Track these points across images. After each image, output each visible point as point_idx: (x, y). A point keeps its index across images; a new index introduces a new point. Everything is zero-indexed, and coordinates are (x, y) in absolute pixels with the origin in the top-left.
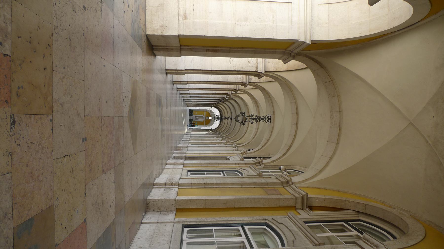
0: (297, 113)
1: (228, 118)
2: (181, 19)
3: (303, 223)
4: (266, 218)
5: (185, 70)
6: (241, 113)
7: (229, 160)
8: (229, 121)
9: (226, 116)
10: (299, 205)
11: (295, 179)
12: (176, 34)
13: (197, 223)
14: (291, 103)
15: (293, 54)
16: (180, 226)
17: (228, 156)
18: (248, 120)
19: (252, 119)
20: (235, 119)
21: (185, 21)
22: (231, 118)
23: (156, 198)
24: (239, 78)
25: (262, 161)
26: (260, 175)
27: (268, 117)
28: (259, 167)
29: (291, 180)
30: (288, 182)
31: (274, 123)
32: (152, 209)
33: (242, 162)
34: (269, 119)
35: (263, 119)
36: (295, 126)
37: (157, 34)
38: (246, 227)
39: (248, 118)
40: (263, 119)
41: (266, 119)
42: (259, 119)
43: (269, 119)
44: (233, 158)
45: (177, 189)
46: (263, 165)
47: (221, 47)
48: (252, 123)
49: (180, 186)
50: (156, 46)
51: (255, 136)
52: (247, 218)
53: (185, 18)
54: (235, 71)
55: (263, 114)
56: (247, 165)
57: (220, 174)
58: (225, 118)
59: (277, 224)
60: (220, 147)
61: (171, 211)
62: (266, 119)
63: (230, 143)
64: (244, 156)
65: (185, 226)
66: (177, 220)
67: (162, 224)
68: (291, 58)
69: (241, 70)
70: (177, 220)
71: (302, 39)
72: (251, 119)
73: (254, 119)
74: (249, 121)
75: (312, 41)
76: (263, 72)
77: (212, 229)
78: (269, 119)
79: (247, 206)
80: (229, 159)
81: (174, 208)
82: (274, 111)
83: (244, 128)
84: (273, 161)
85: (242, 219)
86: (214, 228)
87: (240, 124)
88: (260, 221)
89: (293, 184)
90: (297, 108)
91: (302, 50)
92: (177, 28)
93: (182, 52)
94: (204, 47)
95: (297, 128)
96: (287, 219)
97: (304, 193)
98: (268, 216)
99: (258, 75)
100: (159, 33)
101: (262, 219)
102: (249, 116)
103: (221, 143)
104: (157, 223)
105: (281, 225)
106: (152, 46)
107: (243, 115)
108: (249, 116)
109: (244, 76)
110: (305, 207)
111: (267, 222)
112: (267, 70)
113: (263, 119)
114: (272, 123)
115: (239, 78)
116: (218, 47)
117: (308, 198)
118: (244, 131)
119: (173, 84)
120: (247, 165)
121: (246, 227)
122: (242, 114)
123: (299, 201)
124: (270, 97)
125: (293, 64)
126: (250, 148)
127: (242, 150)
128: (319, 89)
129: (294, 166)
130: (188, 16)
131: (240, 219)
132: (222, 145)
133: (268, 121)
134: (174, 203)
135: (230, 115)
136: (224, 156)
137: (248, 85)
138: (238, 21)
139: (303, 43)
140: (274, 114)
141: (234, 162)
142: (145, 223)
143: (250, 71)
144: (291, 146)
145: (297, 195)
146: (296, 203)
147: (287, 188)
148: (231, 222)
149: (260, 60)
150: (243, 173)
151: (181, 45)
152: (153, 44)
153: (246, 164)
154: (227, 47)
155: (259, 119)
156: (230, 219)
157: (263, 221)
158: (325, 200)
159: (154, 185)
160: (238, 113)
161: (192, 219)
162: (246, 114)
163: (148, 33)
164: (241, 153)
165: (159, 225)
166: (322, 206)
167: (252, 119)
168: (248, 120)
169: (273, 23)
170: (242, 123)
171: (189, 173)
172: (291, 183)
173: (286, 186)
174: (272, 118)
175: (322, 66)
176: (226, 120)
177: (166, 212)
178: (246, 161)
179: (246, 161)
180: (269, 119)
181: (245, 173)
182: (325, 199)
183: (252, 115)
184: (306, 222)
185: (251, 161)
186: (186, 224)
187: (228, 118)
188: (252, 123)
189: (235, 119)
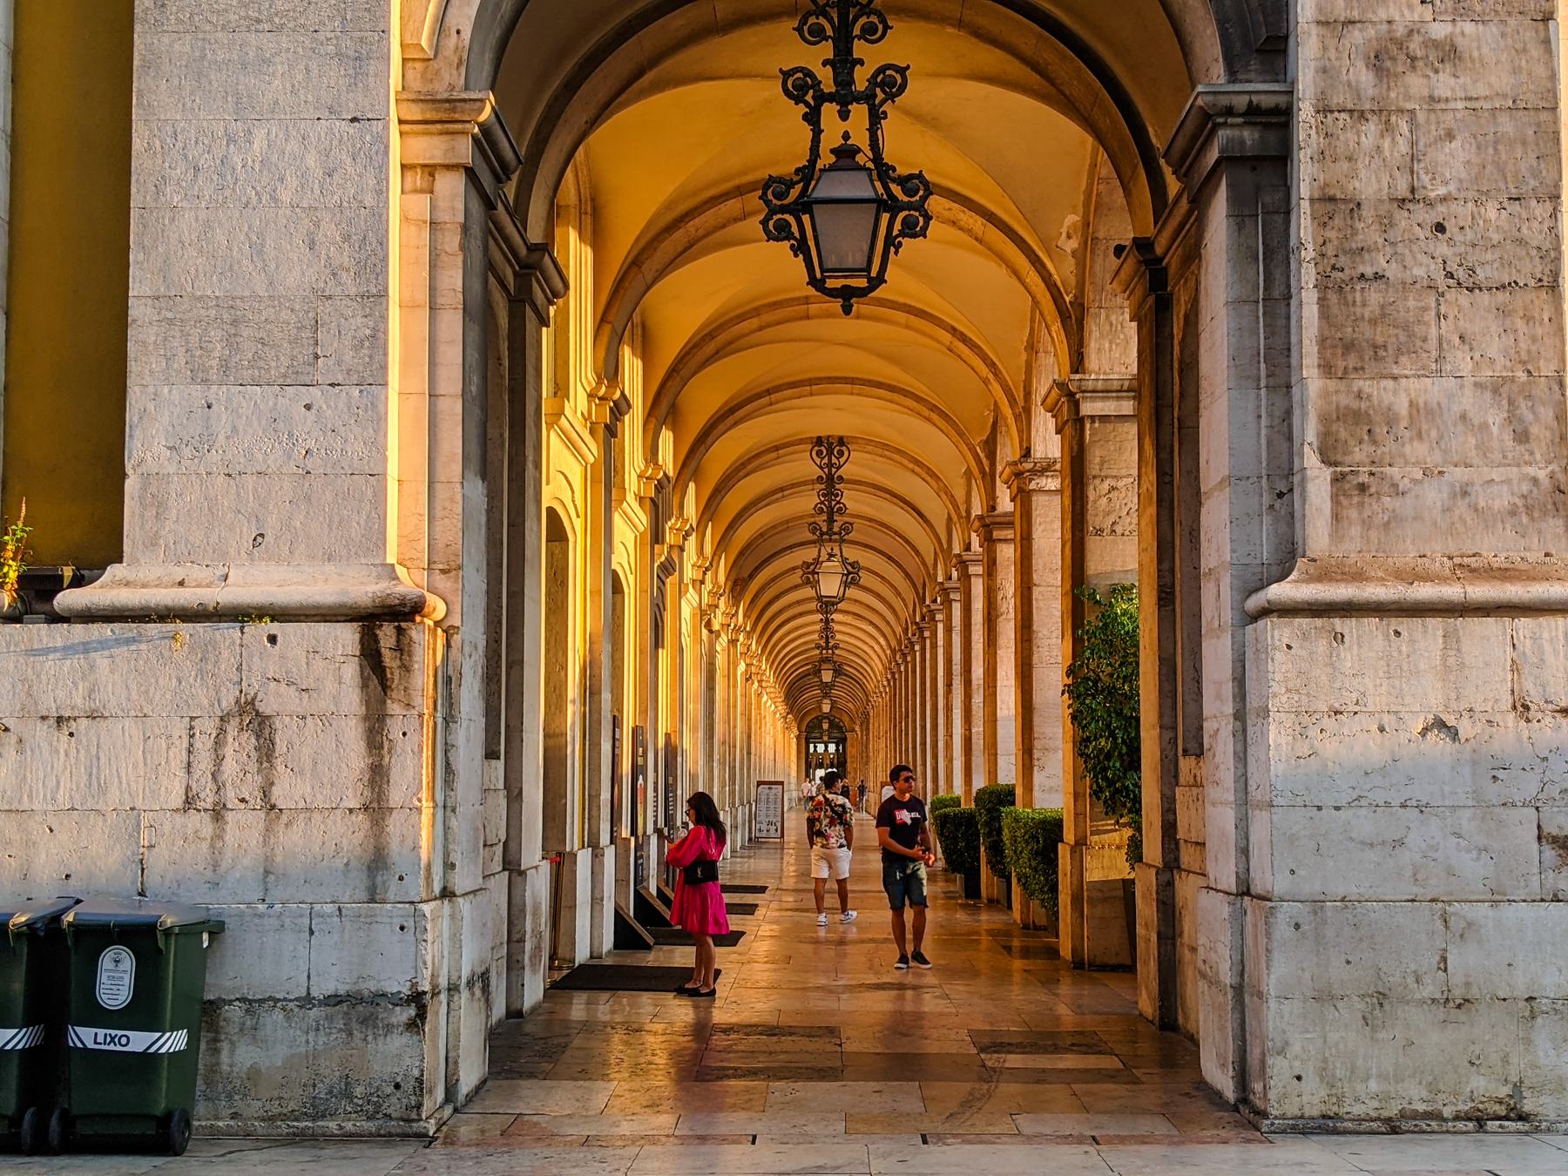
1: (830, 484)
6: (782, 233)
18: (861, 139)
20: (847, 296)
22: (830, 447)
39: (831, 138)
48: (891, 82)
73: (843, 63)
74: (876, 118)
87: (910, 230)
102: (813, 118)
108: (813, 118)
168: (861, 139)
183: (799, 86)
189: (847, 296)
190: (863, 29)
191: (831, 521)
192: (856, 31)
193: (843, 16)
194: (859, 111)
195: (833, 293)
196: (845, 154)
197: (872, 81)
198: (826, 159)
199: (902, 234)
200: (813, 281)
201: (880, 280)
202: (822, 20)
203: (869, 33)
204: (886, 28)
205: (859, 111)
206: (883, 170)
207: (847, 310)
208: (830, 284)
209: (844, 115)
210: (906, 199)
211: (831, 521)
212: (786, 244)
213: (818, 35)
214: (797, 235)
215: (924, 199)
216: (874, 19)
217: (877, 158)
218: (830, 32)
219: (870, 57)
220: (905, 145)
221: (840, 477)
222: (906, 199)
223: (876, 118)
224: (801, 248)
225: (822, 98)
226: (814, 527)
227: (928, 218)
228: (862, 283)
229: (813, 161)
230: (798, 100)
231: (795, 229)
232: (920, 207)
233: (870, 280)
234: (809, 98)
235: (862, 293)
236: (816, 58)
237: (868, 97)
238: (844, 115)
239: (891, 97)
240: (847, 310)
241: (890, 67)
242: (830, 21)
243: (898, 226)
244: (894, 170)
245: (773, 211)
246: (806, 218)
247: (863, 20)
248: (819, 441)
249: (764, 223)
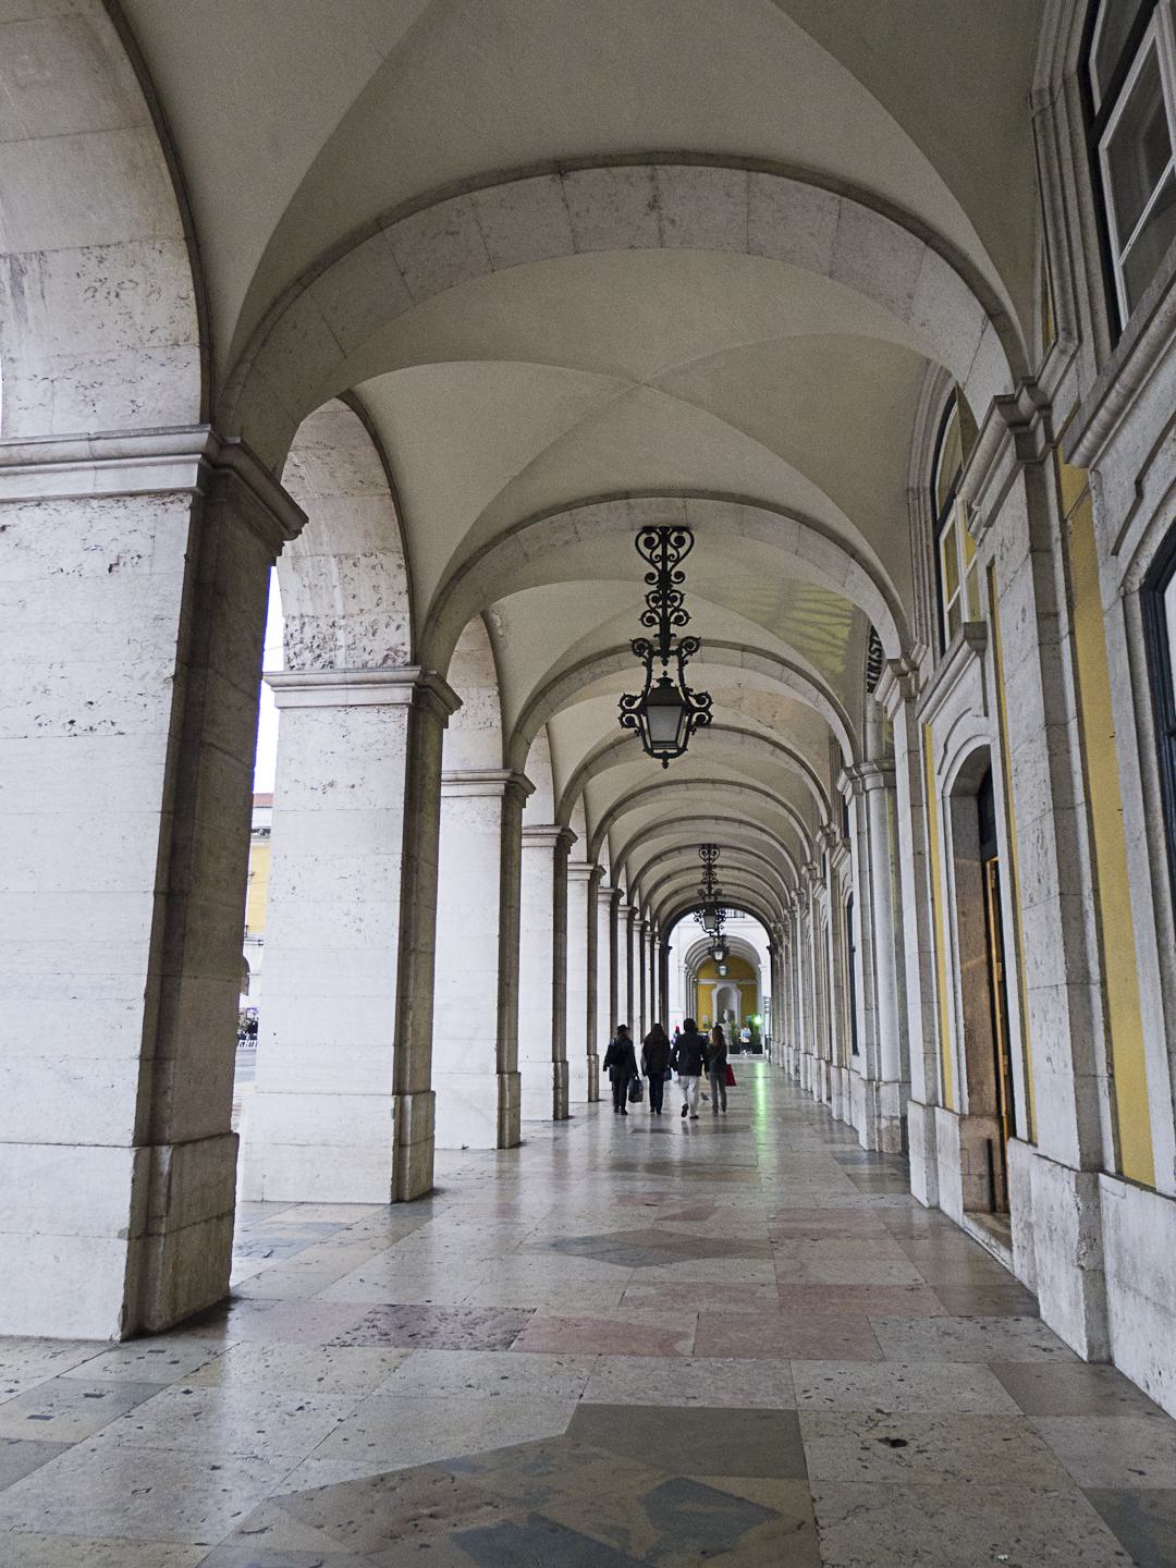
0: (561, 167)
1: (709, 868)
6: (631, 723)
9: (699, 876)
18: (673, 674)
20: (665, 757)
22: (709, 849)
27: (649, 543)
31: (687, 493)
34: (664, 539)
35: (665, 574)
39: (658, 673)
40: (665, 574)
41: (664, 558)
43: (664, 540)
48: (691, 645)
58: (710, 880)
60: (865, 872)
62: (664, 558)
63: (835, 827)
73: (665, 636)
74: (682, 663)
78: (664, 539)
87: (701, 722)
90: (519, 173)
95: (684, 157)
102: (648, 665)
103: (835, 877)
108: (648, 665)
118: (765, 754)
119: (431, 1192)
133: (680, 541)
135: (695, 858)
168: (673, 674)
176: (720, 875)
180: (664, 540)
187: (709, 868)
188: (691, 645)
189: (665, 757)
190: (676, 618)
191: (710, 889)
192: (672, 619)
193: (665, 611)
194: (673, 661)
195: (658, 756)
196: (665, 681)
197: (681, 647)
198: (654, 684)
199: (696, 724)
200: (647, 749)
201: (684, 748)
202: (653, 615)
203: (678, 621)
204: (688, 618)
205: (673, 660)
206: (687, 691)
207: (665, 765)
208: (655, 751)
209: (665, 663)
210: (697, 706)
211: (710, 889)
212: (632, 730)
213: (651, 621)
214: (638, 725)
215: (708, 706)
216: (681, 613)
217: (682, 684)
218: (657, 620)
220: (699, 675)
221: (715, 866)
222: (697, 706)
223: (682, 663)
224: (641, 732)
225: (652, 654)
226: (701, 892)
227: (711, 717)
228: (675, 751)
229: (648, 686)
230: (640, 655)
231: (637, 722)
232: (705, 710)
233: (678, 748)
234: (646, 654)
235: (673, 756)
237: (678, 653)
238: (665, 663)
239: (690, 653)
240: (665, 765)
241: (688, 638)
242: (657, 614)
243: (694, 719)
244: (692, 690)
245: (625, 712)
246: (644, 719)
247: (676, 614)
248: (703, 846)
249: (620, 719)
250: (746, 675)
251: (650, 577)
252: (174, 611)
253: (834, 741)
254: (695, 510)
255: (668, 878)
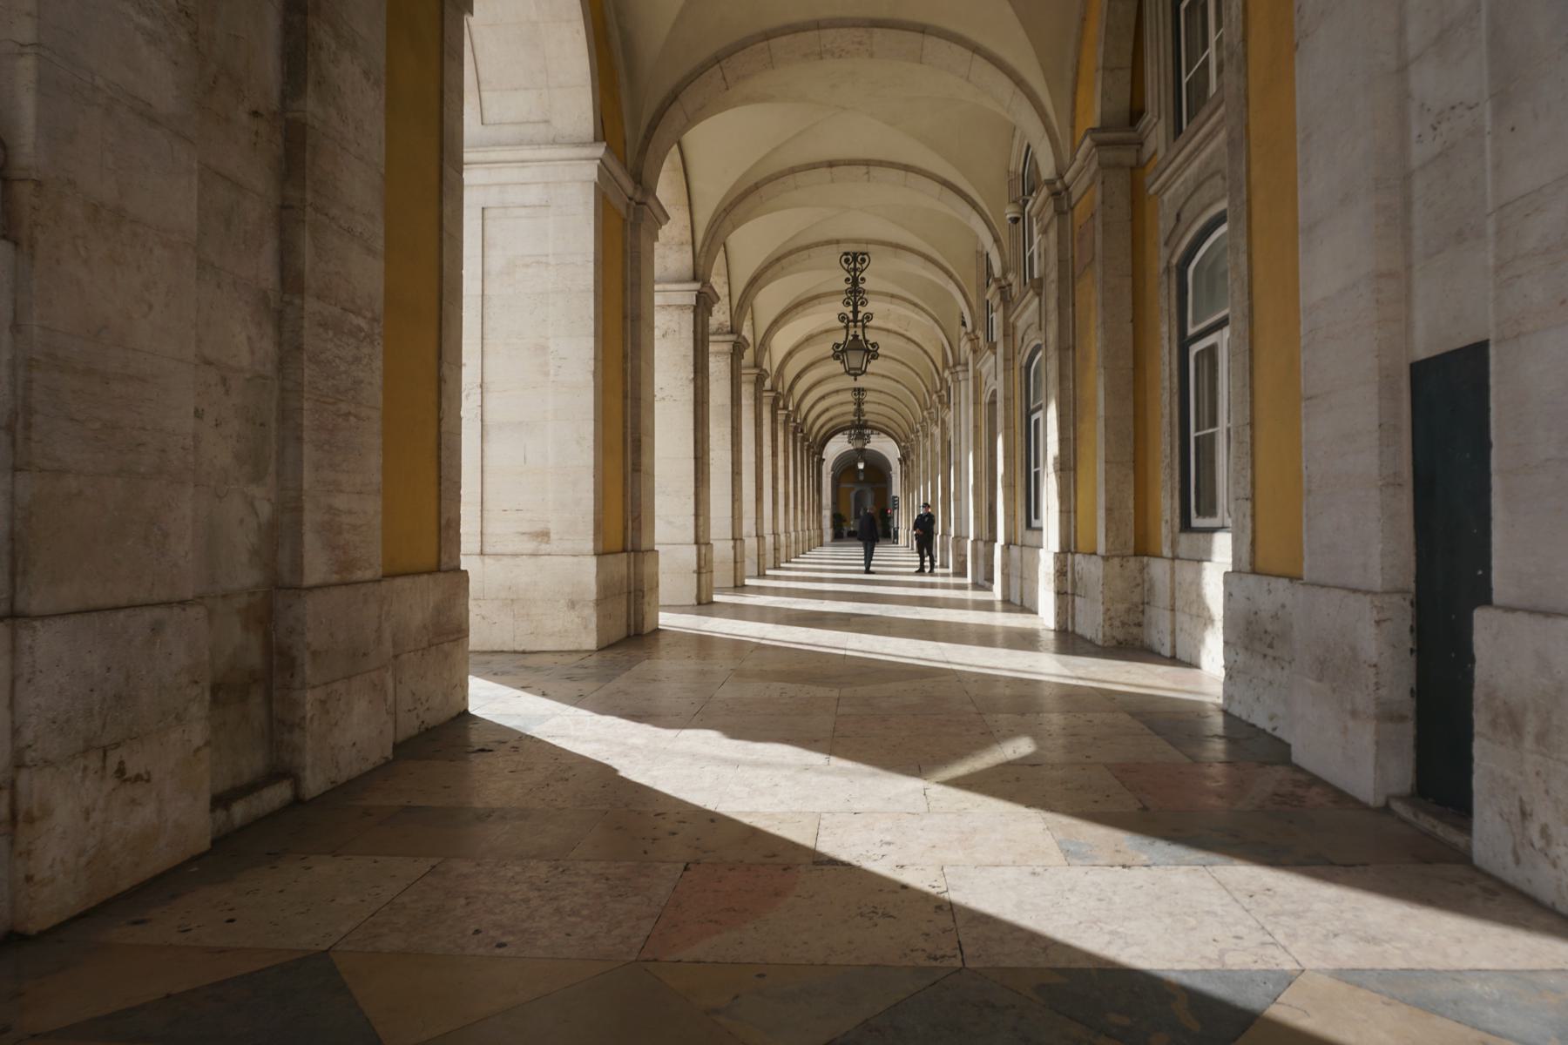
0: (831, 164)
1: (859, 403)
2: (544, 548)
3: (1182, 139)
4: (1163, 265)
5: (697, 543)
7: (994, 392)
8: (869, 397)
9: (852, 408)
10: (1128, 156)
11: (1047, 169)
12: (591, 563)
13: (1177, 486)
14: (796, 188)
15: (638, 197)
16: (1184, 539)
17: (985, 398)
18: (859, 332)
19: (855, 320)
20: (855, 375)
21: (553, 536)
23: (1100, 618)
24: (718, 367)
25: (996, 280)
26: (1038, 286)
27: (847, 261)
28: (1015, 289)
29: (1050, 183)
30: (1056, 195)
32: (1135, 630)
33: (1000, 349)
34: (855, 261)
36: (877, 172)
37: (594, 620)
38: (1191, 331)
39: (852, 332)
40: (855, 281)
41: (855, 269)
42: (855, 293)
43: (855, 259)
44: (991, 379)
45: (1078, 557)
46: (1011, 277)
47: (625, 427)
48: (869, 317)
49: (1069, 545)
50: (629, 626)
51: (916, 305)
52: (1164, 329)
53: (544, 535)
54: (695, 379)
55: (838, 279)
56: (1009, 331)
57: (1037, 421)
58: (859, 411)
59: (1182, 227)
60: (957, 426)
61: (1142, 569)
62: (855, 269)
64: (981, 342)
65: (1186, 526)
66: (1166, 552)
67: (1177, 594)
68: (651, 202)
69: (691, 359)
70: (1166, 552)
71: (591, 171)
72: (855, 321)
73: (855, 312)
74: (864, 327)
75: (596, 140)
76: (697, 286)
77: (1197, 439)
78: (855, 261)
79: (1129, 327)
80: (994, 393)
81: (1133, 564)
82: (829, 242)
83: (886, 344)
84: (997, 240)
85: (1165, 342)
86: (1193, 435)
87: (874, 358)
88: (1174, 286)
89: (1061, 177)
91: (625, 165)
92: (575, 559)
93: (644, 546)
94: (625, 479)
96: (1166, 197)
97: (1087, 142)
98: (1160, 259)
99: (703, 304)
100: (591, 614)
101: (1165, 278)
102: (847, 327)
103: (943, 422)
104: (1173, 610)
105: (1183, 216)
106: (628, 636)
107: (843, 351)
108: (847, 327)
109: (712, 348)
110: (1132, 135)
111: (1174, 261)
112: (690, 273)
113: (855, 281)
114: (871, 248)
115: (718, 367)
116: (625, 434)
117: (1104, 128)
118: (902, 343)
120: (1009, 331)
121: (1191, 331)
122: (839, 353)
123: (1111, 155)
124: (778, 260)
125: (667, 189)
126: (958, 322)
127: (965, 348)
128: (748, 100)
129: (1012, 168)
130: (538, 527)
131: (1166, 350)
132: (950, 416)
133: (863, 260)
134: (1116, 561)
135: (849, 396)
136: (984, 411)
137: (739, 334)
138: (547, 374)
139: (603, 167)
140: (838, 242)
141: (1001, 377)
142: (1174, 647)
143: (695, 332)
144: (945, 183)
145: (1094, 166)
146: (1119, 166)
147: (1076, 193)
148: (1176, 380)
149: (658, 299)
150: (1034, 344)
151: (624, 550)
152: (622, 633)
153: (1005, 335)
154: (625, 406)
155: (855, 293)
156: (1167, 384)
157: (1174, 276)
158: (1108, 69)
159: (1066, 630)
160: (837, 367)
161: (1166, 505)
162: (840, 338)
163: (590, 642)
164: (975, 351)
165: (1178, 604)
166: (1128, 78)
167: (855, 320)
168: (859, 332)
169: (547, 264)
170: (871, 352)
171: (1035, 523)
172: (1058, 185)
173: (1069, 199)
174: (852, 248)
175: (674, 97)
176: (866, 407)
177: (1146, 586)
178: (997, 335)
179: (997, 335)
180: (855, 259)
181: (1034, 339)
182: (1104, 68)
183: (842, 317)
184: (1178, 130)
185: (997, 318)
186: (1177, 521)
187: (859, 403)
189: (855, 375)
196: (855, 337)
219: (863, 310)
220: (872, 337)
223: (864, 327)
236: (848, 310)
250: (892, 307)
251: (847, 280)
252: (691, 353)
253: (944, 350)
254: (871, 248)
255: (827, 410)
